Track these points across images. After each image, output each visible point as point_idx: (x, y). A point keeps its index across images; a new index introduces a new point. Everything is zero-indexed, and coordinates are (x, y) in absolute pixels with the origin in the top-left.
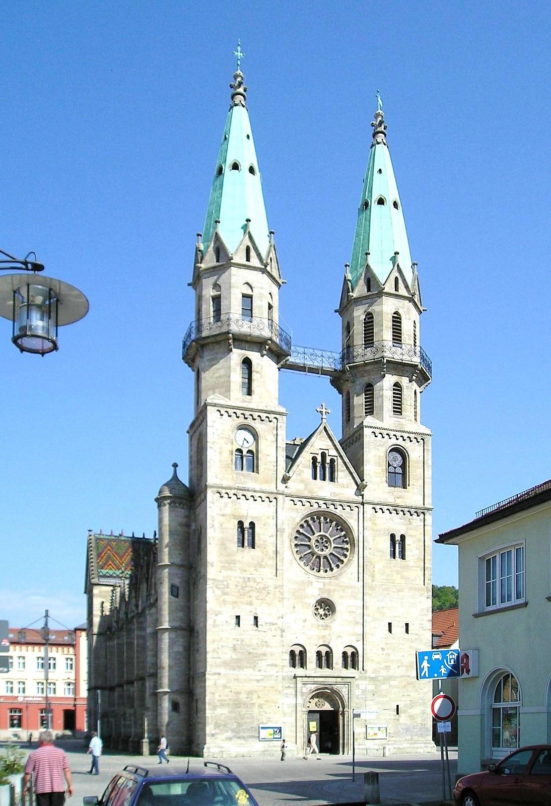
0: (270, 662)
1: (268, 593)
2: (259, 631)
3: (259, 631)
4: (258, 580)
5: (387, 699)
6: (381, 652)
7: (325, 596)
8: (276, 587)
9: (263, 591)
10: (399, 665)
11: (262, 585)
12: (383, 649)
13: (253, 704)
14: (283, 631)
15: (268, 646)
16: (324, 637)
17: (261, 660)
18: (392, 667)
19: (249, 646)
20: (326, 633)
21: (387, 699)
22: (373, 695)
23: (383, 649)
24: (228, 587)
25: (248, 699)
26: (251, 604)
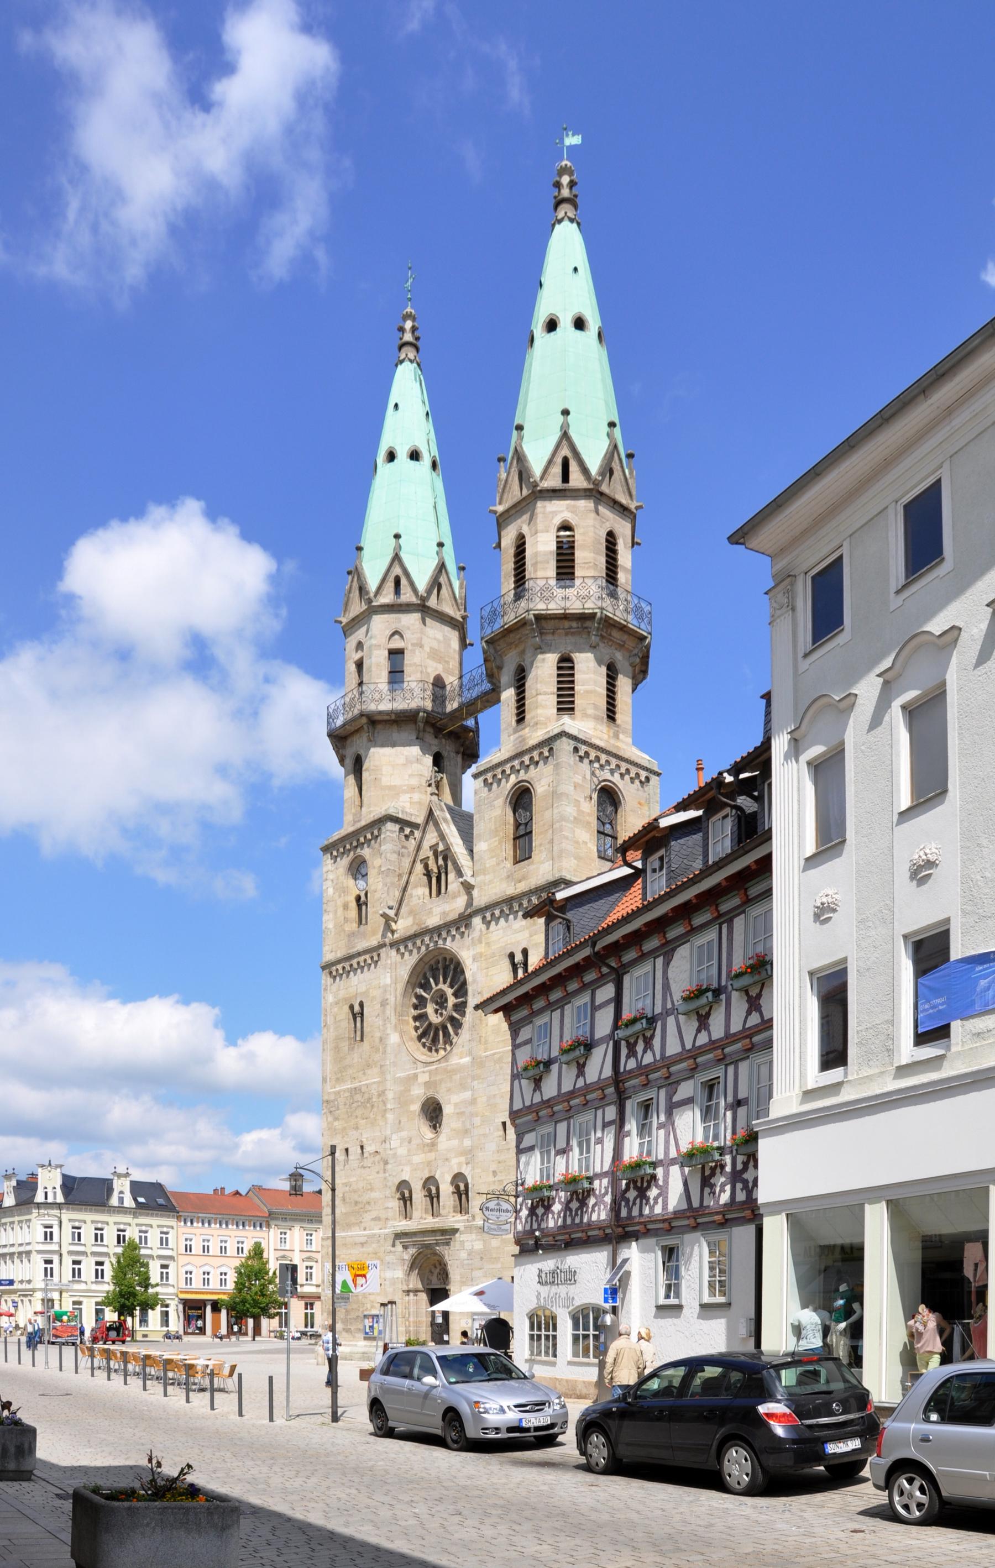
0: (374, 1214)
1: (373, 1106)
4: (364, 1089)
5: (499, 1266)
6: (491, 1179)
7: (429, 1094)
8: (379, 1095)
11: (366, 1096)
12: (495, 1173)
14: (386, 1163)
15: (372, 1189)
16: (429, 1163)
19: (355, 1191)
20: (432, 1156)
21: (499, 1266)
22: (482, 1258)
23: (495, 1173)
24: (338, 1109)
26: (357, 1128)
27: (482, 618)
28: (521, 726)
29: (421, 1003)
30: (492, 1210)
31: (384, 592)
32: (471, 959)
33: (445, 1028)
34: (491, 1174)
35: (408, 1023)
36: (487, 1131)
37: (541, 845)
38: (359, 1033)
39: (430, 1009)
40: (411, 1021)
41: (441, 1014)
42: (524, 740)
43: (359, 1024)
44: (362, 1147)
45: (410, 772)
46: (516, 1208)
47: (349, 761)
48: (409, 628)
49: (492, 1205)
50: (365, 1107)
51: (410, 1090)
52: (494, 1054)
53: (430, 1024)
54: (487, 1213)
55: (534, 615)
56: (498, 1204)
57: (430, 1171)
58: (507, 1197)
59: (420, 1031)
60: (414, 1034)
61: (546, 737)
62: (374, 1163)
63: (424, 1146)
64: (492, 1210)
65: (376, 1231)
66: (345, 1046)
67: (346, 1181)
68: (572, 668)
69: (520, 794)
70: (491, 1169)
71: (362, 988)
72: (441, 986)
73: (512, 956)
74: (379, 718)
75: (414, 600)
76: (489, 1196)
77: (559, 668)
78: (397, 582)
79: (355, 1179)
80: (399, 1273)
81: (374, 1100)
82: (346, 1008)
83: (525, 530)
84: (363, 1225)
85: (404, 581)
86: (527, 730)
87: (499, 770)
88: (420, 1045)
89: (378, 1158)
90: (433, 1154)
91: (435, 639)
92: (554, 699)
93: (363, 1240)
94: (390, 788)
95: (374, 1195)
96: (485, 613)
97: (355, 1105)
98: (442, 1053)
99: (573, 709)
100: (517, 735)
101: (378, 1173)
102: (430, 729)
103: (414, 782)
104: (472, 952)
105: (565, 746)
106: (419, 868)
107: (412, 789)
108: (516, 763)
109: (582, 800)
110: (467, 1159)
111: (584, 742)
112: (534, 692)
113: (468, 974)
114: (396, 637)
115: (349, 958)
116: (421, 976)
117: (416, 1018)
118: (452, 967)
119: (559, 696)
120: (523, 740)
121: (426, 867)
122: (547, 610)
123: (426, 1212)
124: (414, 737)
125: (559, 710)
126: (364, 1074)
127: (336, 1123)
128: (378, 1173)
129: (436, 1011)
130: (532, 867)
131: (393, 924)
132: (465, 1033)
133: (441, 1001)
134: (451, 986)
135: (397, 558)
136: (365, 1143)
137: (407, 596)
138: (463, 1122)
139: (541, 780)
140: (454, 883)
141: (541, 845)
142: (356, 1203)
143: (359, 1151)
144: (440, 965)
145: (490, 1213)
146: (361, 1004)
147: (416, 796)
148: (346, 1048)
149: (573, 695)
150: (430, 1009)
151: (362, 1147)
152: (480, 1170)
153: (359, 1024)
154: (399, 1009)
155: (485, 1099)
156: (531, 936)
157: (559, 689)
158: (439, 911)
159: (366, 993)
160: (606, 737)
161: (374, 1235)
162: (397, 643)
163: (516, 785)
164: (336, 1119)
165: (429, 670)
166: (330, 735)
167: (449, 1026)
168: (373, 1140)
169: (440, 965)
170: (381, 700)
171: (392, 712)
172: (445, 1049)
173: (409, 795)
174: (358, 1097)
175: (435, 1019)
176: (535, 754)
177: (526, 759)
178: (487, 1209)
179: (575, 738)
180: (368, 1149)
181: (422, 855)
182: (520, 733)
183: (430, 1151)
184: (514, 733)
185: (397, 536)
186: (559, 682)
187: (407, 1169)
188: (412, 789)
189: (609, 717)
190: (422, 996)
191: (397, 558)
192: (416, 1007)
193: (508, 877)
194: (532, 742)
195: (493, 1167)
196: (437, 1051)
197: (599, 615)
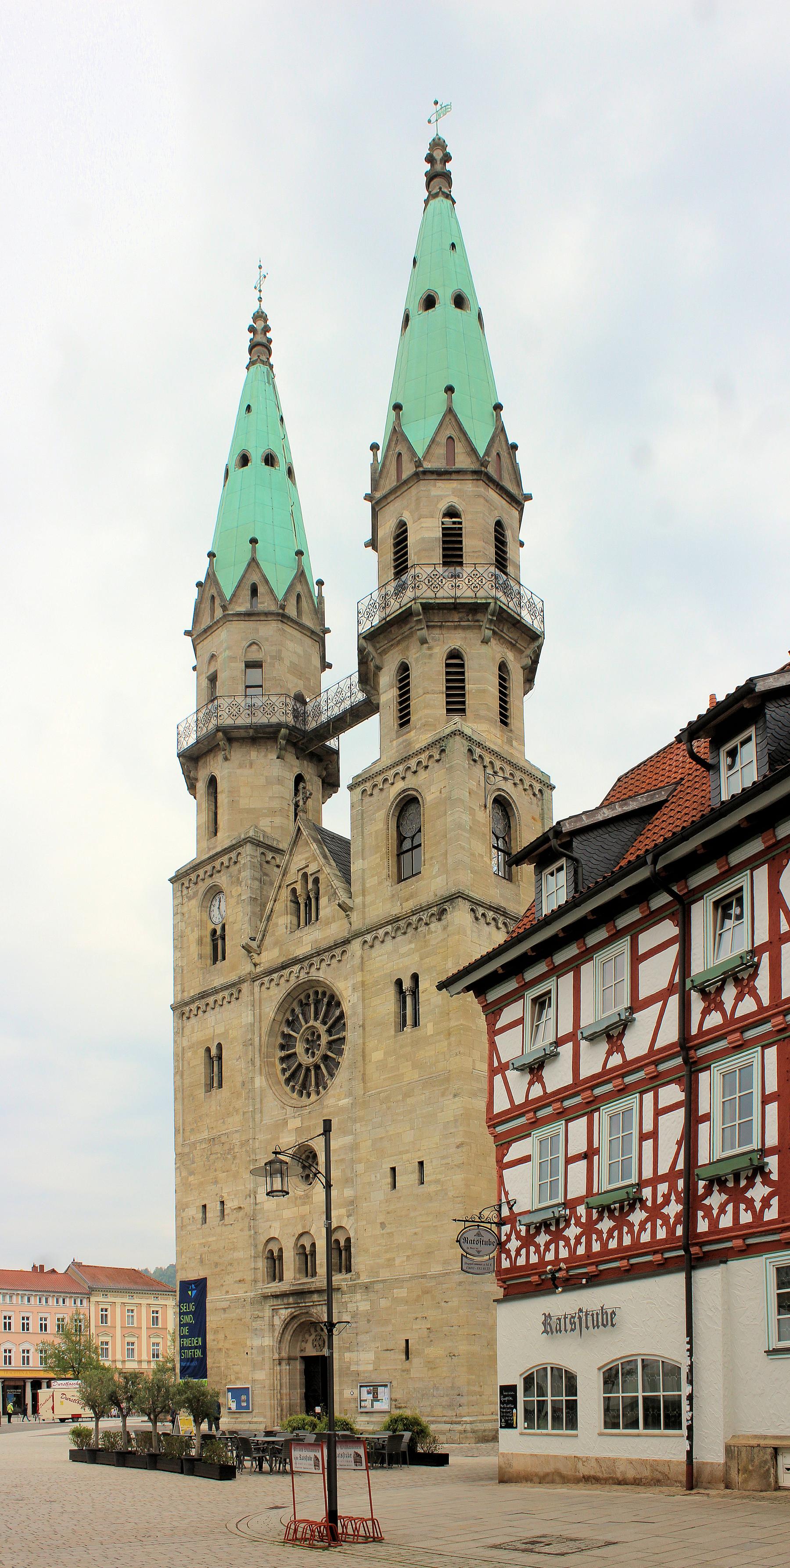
1: (234, 1158)
2: (226, 1225)
3: (226, 1225)
8: (242, 1145)
9: (229, 1156)
10: (409, 1253)
11: (227, 1147)
12: (383, 1225)
13: (220, 1349)
15: (234, 1249)
16: (303, 1217)
17: (228, 1274)
18: (397, 1262)
20: (306, 1209)
22: (369, 1321)
23: (383, 1225)
24: (193, 1162)
25: (215, 1343)
26: (216, 1182)
27: (359, 613)
28: (405, 729)
29: (287, 1042)
30: (472, 1242)
31: (240, 601)
32: (350, 989)
33: (317, 1067)
34: (379, 1226)
35: (274, 1065)
36: (373, 1179)
37: (432, 858)
38: (216, 1079)
39: (299, 1048)
40: (277, 1062)
41: (313, 1054)
42: (409, 744)
43: (216, 1069)
44: (222, 1203)
45: (271, 795)
46: (499, 1238)
47: (201, 786)
48: (267, 640)
49: (471, 1235)
50: (225, 1159)
51: (278, 1138)
52: (380, 1093)
53: (300, 1065)
54: (465, 1246)
55: (421, 604)
56: (478, 1234)
57: (304, 1227)
58: (488, 1225)
59: (287, 1074)
60: (283, 1078)
61: (437, 737)
62: (237, 1220)
63: (296, 1199)
64: (472, 1242)
65: (241, 1294)
66: (201, 1092)
67: (204, 1241)
68: (462, 666)
69: (405, 805)
70: (379, 1221)
71: (220, 1030)
72: (311, 1023)
73: (399, 983)
74: (235, 734)
75: (273, 608)
76: (468, 1224)
77: (447, 665)
78: (254, 591)
79: (214, 1238)
80: (268, 1341)
81: (236, 1150)
82: (202, 1052)
83: (407, 517)
84: (225, 1289)
85: (261, 590)
86: (412, 733)
87: (380, 779)
88: (288, 1089)
89: (241, 1213)
90: (307, 1207)
91: (295, 653)
92: (443, 699)
93: (224, 1305)
94: (249, 811)
95: (240, 1254)
96: (362, 608)
97: (213, 1157)
98: (313, 1097)
99: (463, 711)
100: (401, 740)
101: (242, 1230)
102: (291, 749)
103: (276, 804)
104: (350, 983)
105: (458, 746)
106: (285, 893)
107: (273, 812)
108: (401, 768)
109: (477, 809)
110: (348, 1211)
111: (479, 745)
112: (420, 691)
113: (346, 1007)
114: (254, 647)
115: (203, 995)
116: (289, 1012)
117: (283, 1060)
118: (326, 1000)
119: (448, 696)
120: (409, 744)
121: (294, 891)
122: (436, 598)
123: (300, 1272)
124: (275, 757)
125: (448, 711)
126: (224, 1122)
127: (191, 1178)
128: (242, 1230)
129: (307, 1050)
130: (422, 883)
131: (255, 956)
132: (342, 1074)
133: (312, 1041)
134: (324, 1023)
135: (253, 562)
136: (226, 1198)
137: (265, 604)
138: (343, 1171)
139: (431, 786)
140: (327, 907)
141: (432, 858)
142: (216, 1265)
143: (219, 1207)
144: (311, 1000)
145: (469, 1245)
146: (220, 1046)
147: (278, 821)
148: (203, 1095)
149: (463, 695)
150: (299, 1048)
151: (222, 1203)
152: (365, 1223)
153: (216, 1069)
154: (264, 1050)
155: (369, 1143)
156: (421, 959)
157: (448, 688)
158: (308, 940)
159: (226, 1033)
160: (499, 742)
161: (238, 1299)
162: (254, 655)
163: (400, 794)
164: (192, 1173)
165: (290, 686)
166: (179, 756)
167: (322, 1066)
168: (235, 1195)
169: (311, 1000)
170: (239, 714)
171: (250, 727)
172: (318, 1093)
173: (270, 819)
174: (217, 1148)
175: (306, 1060)
176: (423, 757)
177: (413, 763)
178: (466, 1240)
179: (469, 739)
180: (229, 1205)
181: (290, 879)
182: (405, 737)
183: (304, 1204)
184: (398, 738)
185: (254, 541)
186: (448, 681)
187: (276, 1225)
188: (273, 812)
189: (502, 722)
190: (290, 1035)
191: (253, 562)
192: (282, 1047)
193: (393, 896)
194: (418, 746)
195: (381, 1218)
196: (309, 1095)
197: (492, 605)
